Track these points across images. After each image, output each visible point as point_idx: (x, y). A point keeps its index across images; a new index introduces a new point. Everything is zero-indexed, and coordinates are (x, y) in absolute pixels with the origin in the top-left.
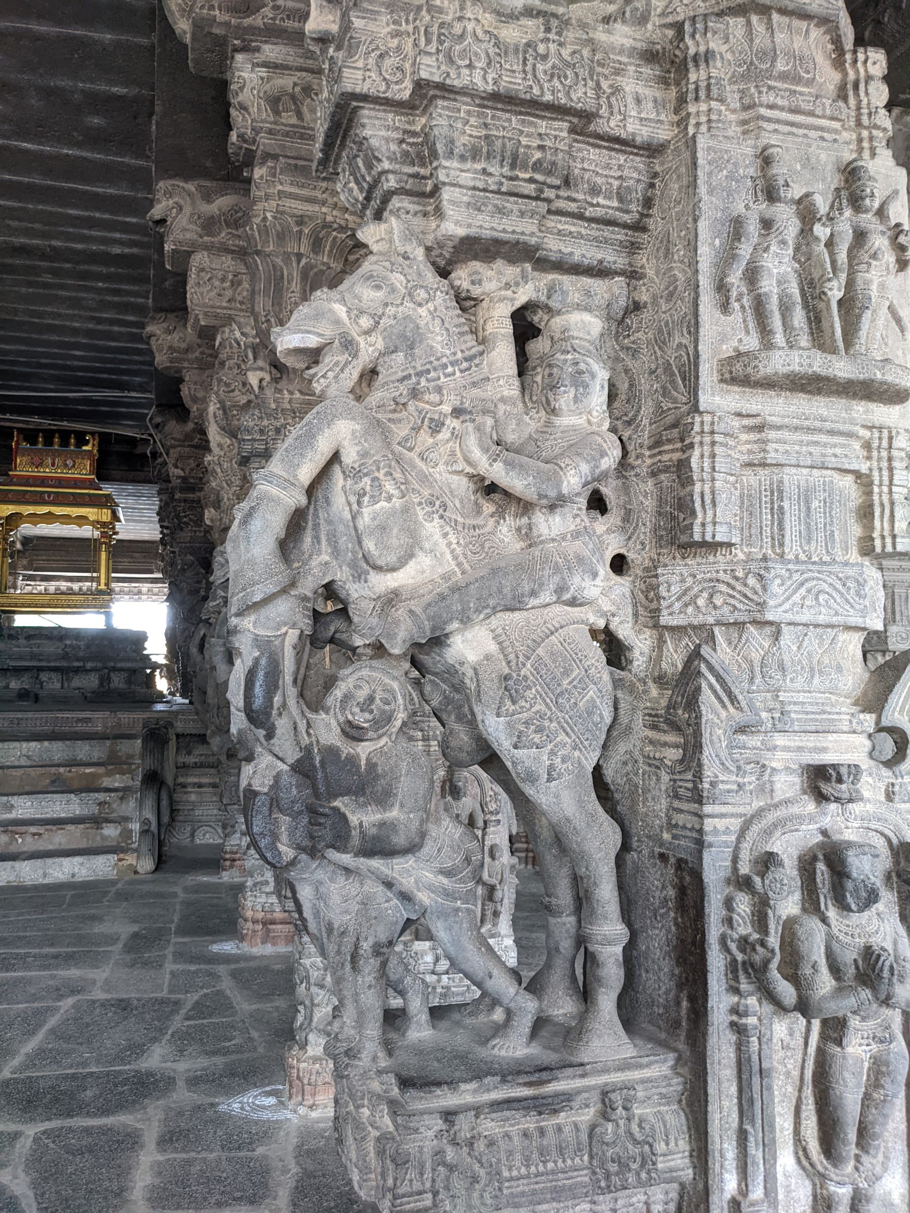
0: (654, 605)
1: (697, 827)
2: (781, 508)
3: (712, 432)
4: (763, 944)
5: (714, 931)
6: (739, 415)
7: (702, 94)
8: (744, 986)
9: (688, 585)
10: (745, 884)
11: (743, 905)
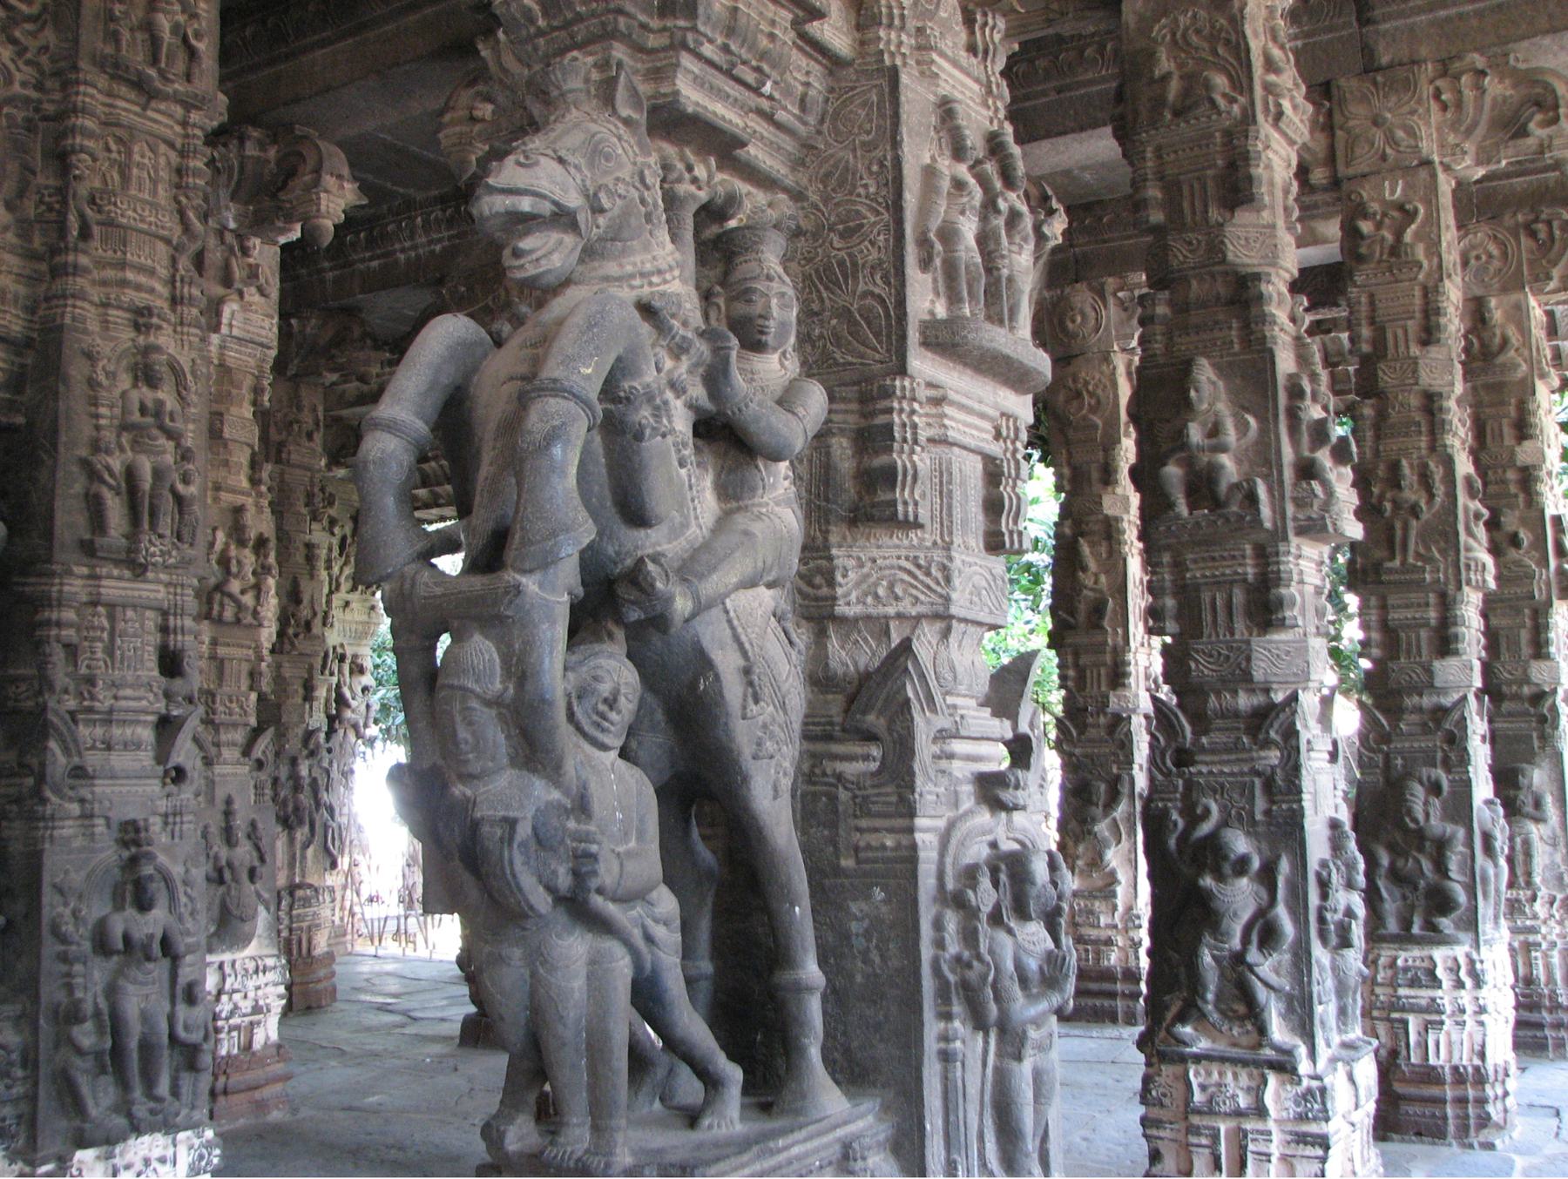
0: (825, 591)
1: (905, 842)
2: (950, 492)
3: (914, 399)
4: (979, 957)
5: (926, 952)
6: (930, 385)
7: (897, 22)
8: (957, 1008)
9: (865, 570)
10: (959, 902)
11: (952, 922)
